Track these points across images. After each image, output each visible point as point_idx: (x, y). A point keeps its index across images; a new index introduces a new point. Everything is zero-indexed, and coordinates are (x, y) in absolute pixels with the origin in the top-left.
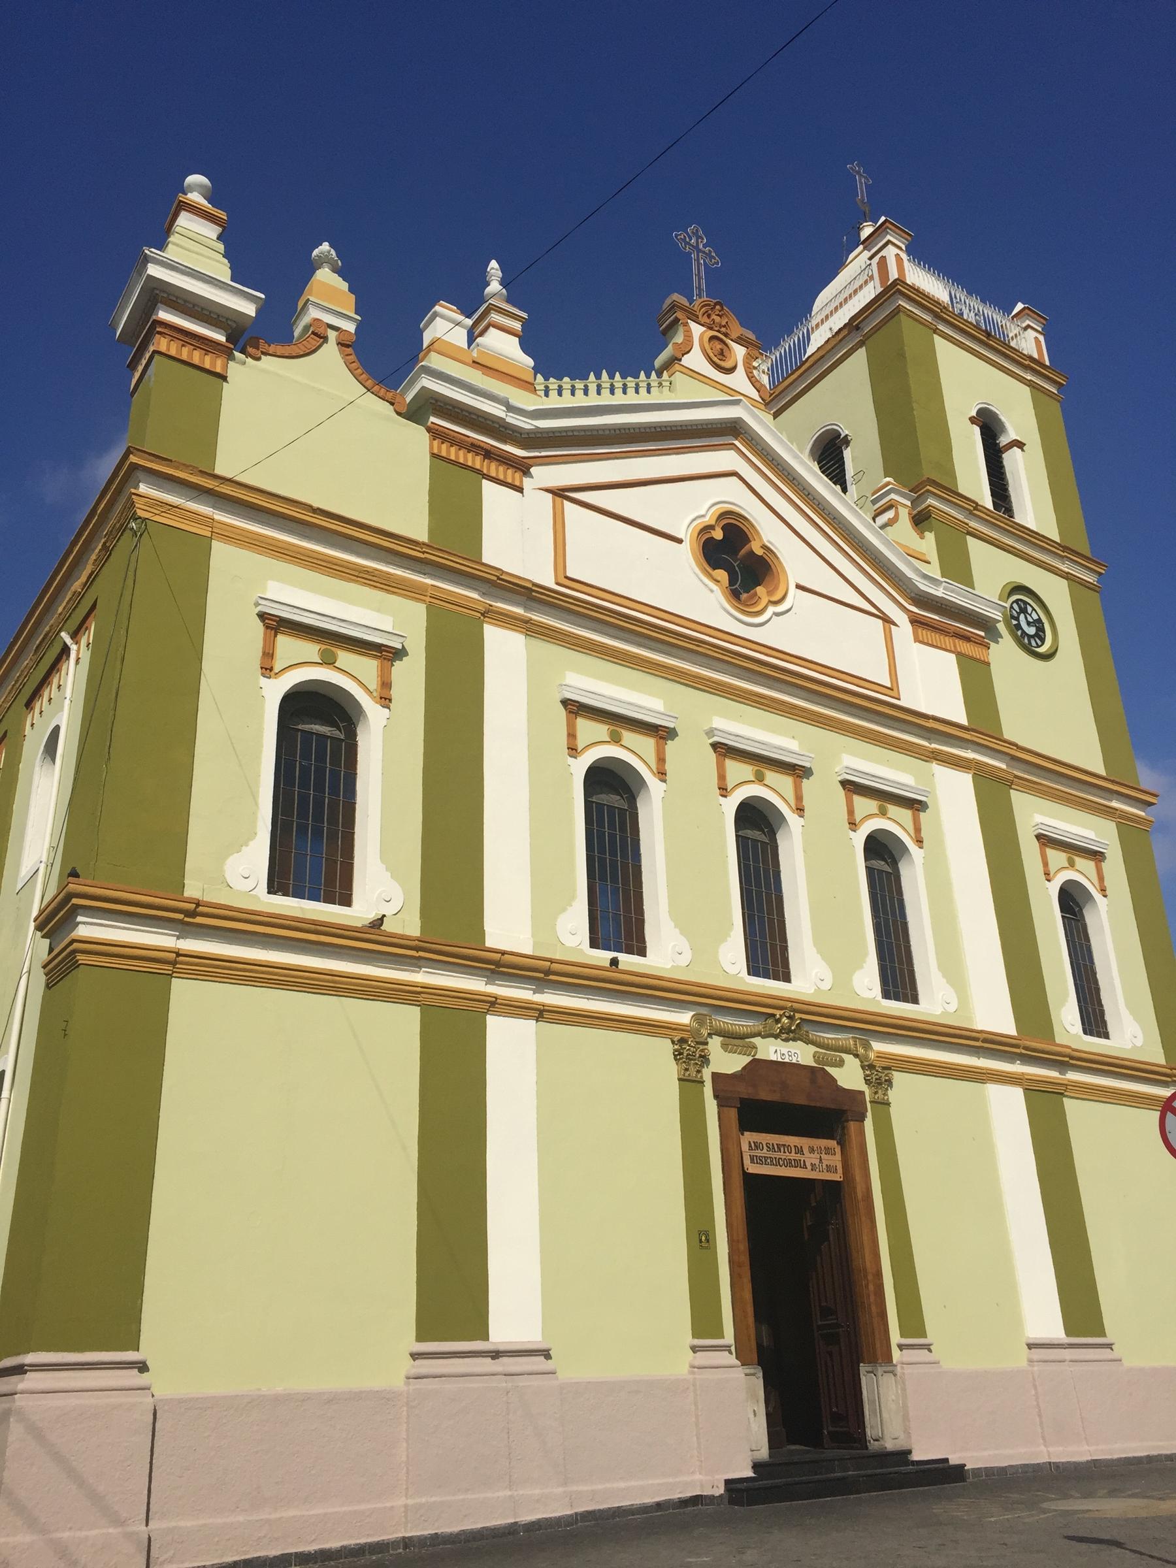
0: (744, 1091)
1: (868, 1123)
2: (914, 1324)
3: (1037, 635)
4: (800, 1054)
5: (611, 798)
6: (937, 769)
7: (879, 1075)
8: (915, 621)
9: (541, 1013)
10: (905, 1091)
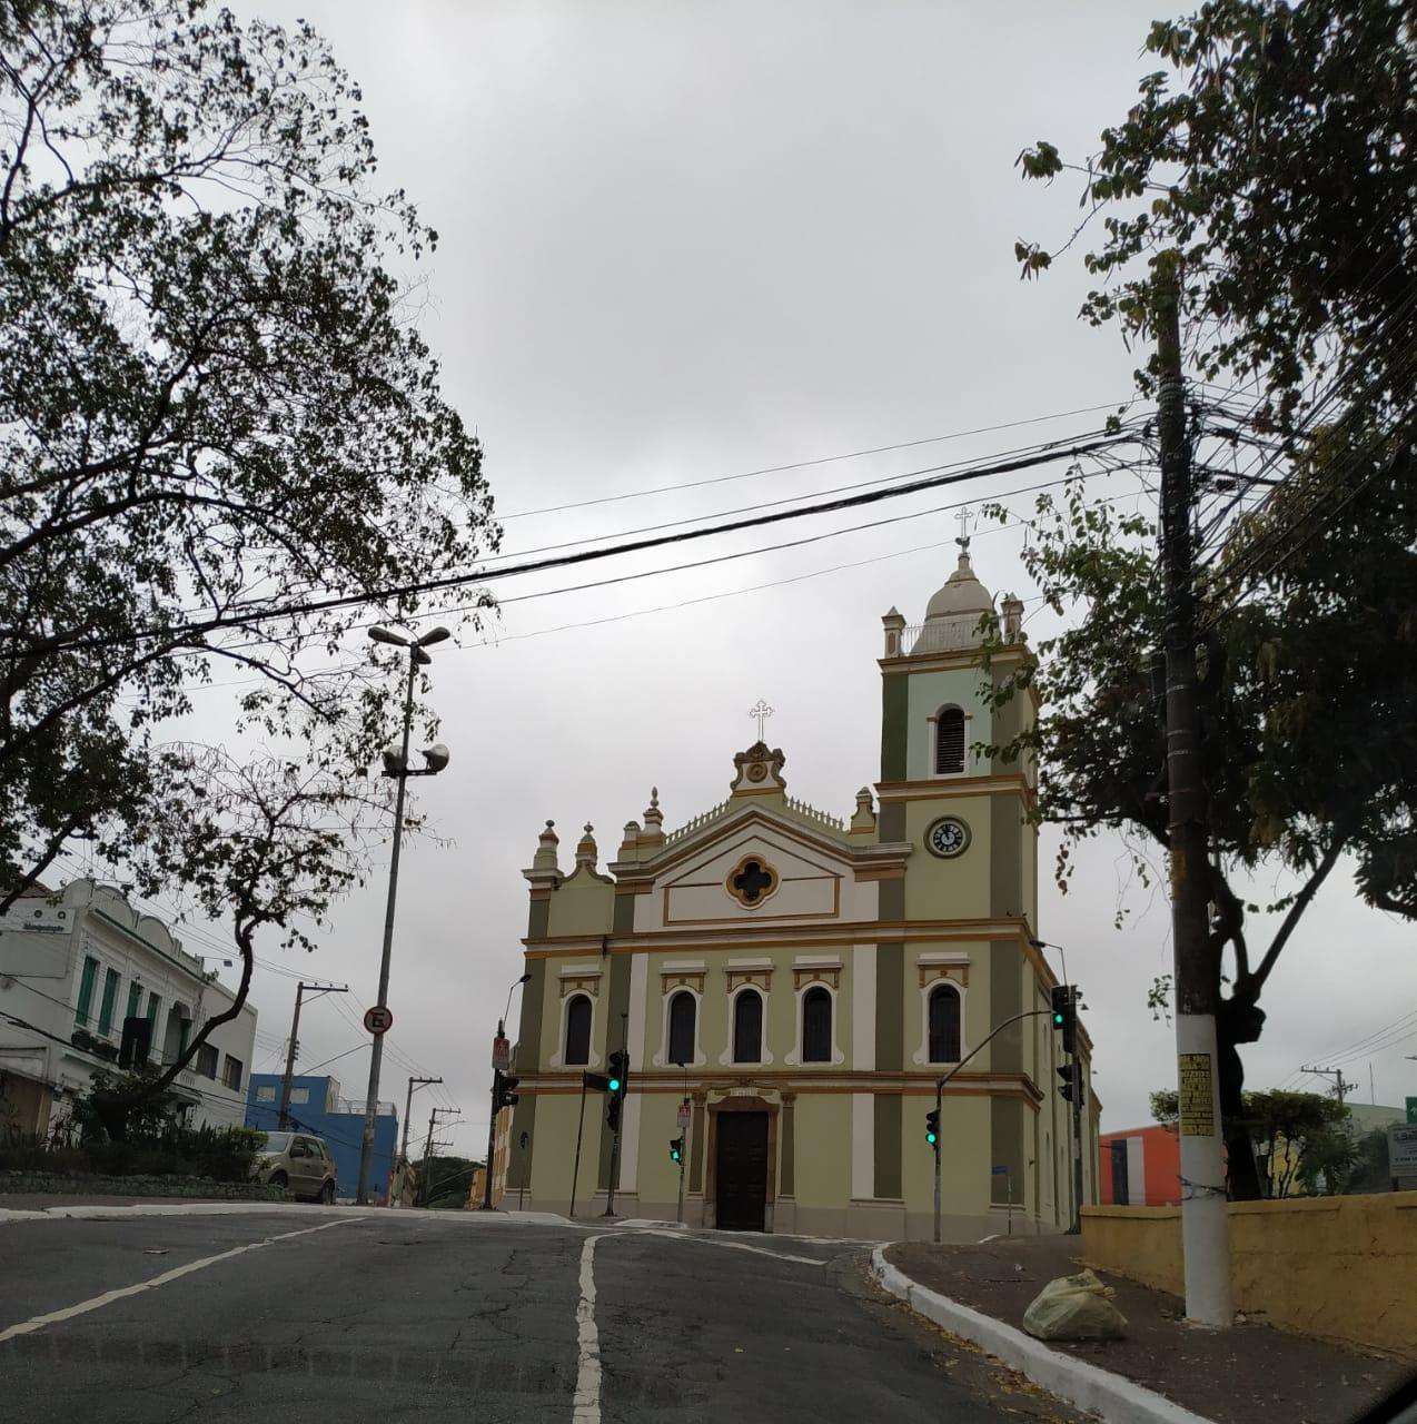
0: (720, 1109)
1: (780, 1118)
2: (788, 1188)
3: (955, 842)
4: (751, 1092)
5: (683, 1008)
6: (857, 947)
7: (789, 1097)
8: (857, 871)
9: (643, 1091)
10: (803, 1104)
